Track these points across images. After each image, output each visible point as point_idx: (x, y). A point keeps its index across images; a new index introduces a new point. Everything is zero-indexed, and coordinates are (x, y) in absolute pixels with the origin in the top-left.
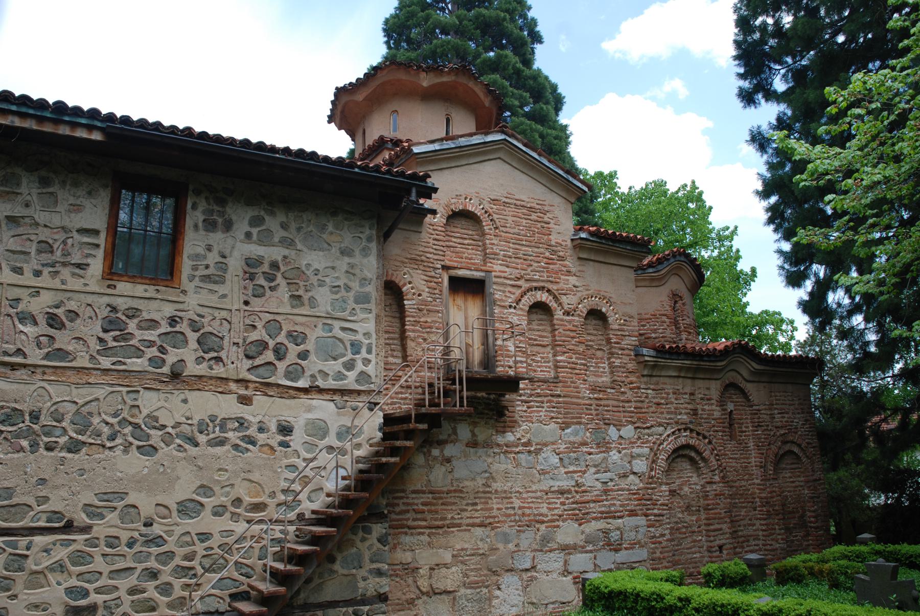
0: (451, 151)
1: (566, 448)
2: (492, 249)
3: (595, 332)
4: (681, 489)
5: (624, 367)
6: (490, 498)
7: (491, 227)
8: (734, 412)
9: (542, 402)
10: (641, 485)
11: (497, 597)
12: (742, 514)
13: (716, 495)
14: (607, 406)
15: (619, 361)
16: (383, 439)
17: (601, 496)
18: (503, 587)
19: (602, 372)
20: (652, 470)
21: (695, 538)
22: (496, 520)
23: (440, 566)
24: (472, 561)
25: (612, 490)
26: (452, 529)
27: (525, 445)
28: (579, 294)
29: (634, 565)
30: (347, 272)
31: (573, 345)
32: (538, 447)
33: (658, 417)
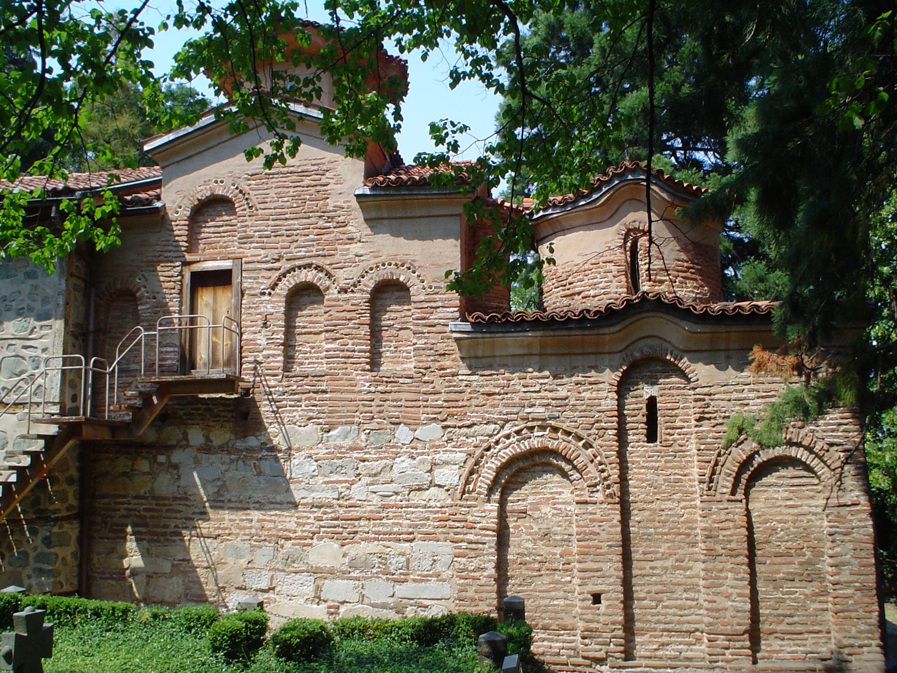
0: (190, 137)
2: (245, 232)
5: (431, 349)
8: (658, 399)
10: (449, 501)
12: (661, 550)
13: (592, 521)
19: (403, 358)
20: (467, 482)
21: (556, 577)
22: (227, 532)
26: (175, 538)
30: (30, 294)
31: (350, 328)
33: (487, 412)
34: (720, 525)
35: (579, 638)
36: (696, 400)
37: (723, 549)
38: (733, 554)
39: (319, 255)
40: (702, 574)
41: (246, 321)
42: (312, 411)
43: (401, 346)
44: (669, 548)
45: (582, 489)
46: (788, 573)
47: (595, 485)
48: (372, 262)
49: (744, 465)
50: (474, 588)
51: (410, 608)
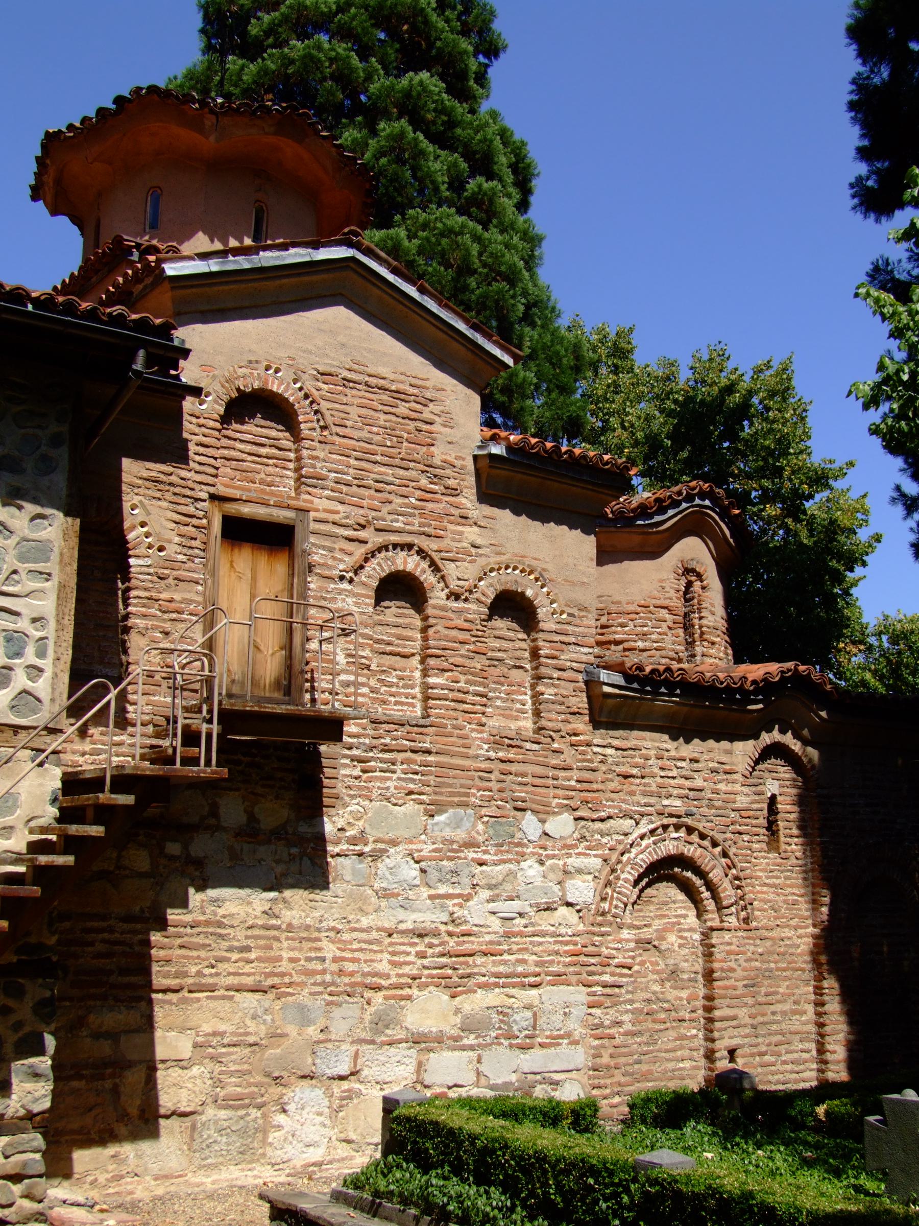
1: (434, 851)
3: (511, 634)
4: (665, 939)
5: (562, 704)
6: (277, 939)
7: (315, 425)
8: (779, 798)
9: (393, 764)
10: (581, 927)
11: (279, 1127)
12: (781, 990)
13: (729, 953)
14: (523, 775)
15: (552, 691)
16: (59, 820)
17: (499, 944)
18: (291, 1107)
19: (519, 711)
21: (683, 1031)
23: (169, 1064)
24: (234, 1057)
25: (521, 934)
27: (353, 841)
28: (481, 561)
29: (557, 1077)
31: (462, 656)
32: (382, 846)
33: (624, 801)
39: (424, 533)
42: (413, 781)
44: (788, 987)
48: (493, 560)
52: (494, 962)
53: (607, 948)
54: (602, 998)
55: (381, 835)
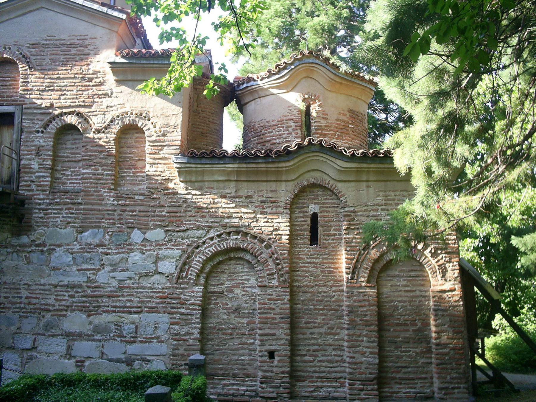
1: (80, 249)
4: (232, 291)
8: (319, 215)
10: (168, 284)
12: (318, 321)
13: (269, 299)
17: (117, 292)
19: (139, 181)
20: (181, 271)
21: (243, 340)
25: (129, 287)
27: (37, 246)
29: (149, 358)
31: (100, 158)
33: (197, 221)
34: (359, 304)
35: (258, 383)
36: (345, 216)
37: (361, 320)
38: (367, 324)
40: (346, 338)
41: (24, 150)
43: (138, 172)
44: (323, 319)
45: (263, 277)
46: (405, 338)
47: (273, 274)
49: (377, 261)
50: (184, 347)
51: (137, 362)
52: (113, 301)
53: (184, 295)
54: (180, 320)
55: (53, 243)
